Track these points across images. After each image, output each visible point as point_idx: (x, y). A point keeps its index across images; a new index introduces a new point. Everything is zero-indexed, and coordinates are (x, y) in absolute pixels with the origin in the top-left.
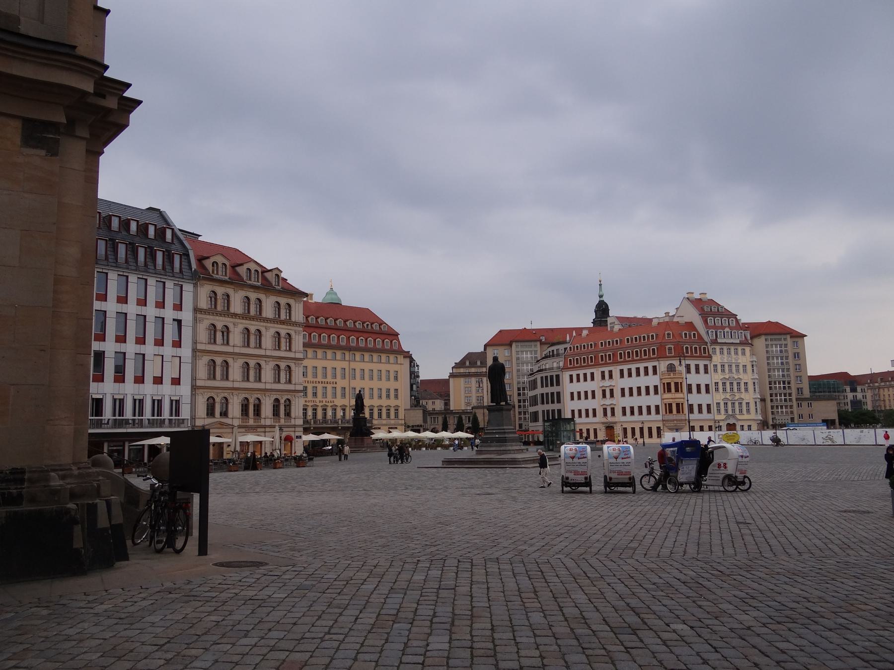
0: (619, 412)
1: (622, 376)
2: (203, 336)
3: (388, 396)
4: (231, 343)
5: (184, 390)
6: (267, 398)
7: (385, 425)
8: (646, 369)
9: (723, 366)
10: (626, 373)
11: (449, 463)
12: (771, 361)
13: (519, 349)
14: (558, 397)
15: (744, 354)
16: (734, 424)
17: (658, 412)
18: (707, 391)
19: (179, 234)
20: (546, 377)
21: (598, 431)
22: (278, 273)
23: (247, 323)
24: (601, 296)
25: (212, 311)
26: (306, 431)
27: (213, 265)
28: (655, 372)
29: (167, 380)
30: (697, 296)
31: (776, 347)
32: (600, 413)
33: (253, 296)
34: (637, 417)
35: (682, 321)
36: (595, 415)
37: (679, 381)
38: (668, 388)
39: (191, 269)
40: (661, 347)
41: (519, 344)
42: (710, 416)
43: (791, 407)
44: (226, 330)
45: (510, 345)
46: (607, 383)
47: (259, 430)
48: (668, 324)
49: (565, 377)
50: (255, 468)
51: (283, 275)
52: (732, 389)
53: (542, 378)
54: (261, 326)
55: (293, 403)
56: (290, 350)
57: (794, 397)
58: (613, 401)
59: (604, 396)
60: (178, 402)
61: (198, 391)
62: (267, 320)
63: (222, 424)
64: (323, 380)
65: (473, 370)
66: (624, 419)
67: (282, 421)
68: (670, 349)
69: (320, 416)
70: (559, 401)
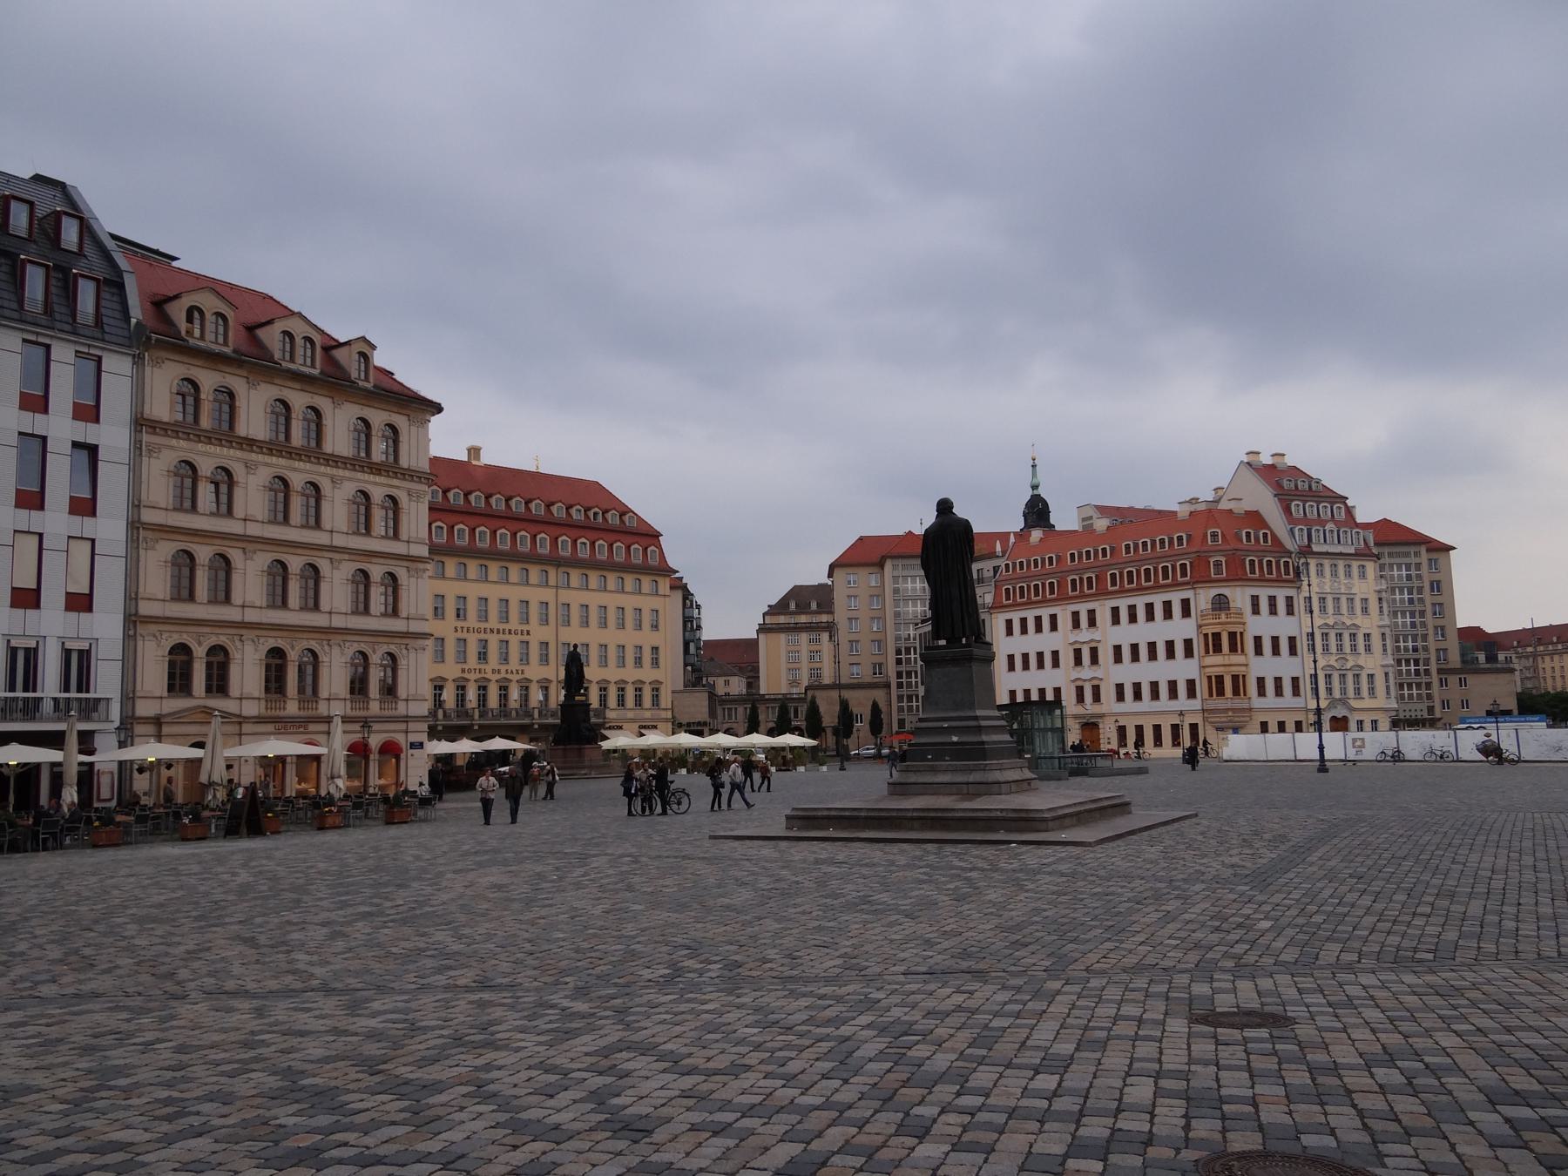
0: (1108, 693)
1: (1116, 620)
2: (159, 488)
3: (638, 662)
4: (239, 510)
5: (104, 627)
6: (336, 651)
7: (633, 720)
10: (1141, 613)
11: (810, 823)
13: (899, 572)
15: (1363, 575)
16: (1345, 719)
17: (1191, 693)
19: (110, 244)
22: (366, 349)
23: (280, 464)
24: (1035, 487)
25: (187, 429)
26: (434, 734)
27: (190, 319)
28: (1186, 612)
29: (53, 597)
30: (1266, 459)
31: (1399, 569)
33: (299, 400)
34: (1146, 704)
37: (1238, 629)
38: (1213, 644)
39: (127, 318)
40: (1200, 561)
41: (900, 562)
43: (1429, 686)
44: (225, 480)
46: (1085, 634)
47: (312, 727)
48: (1208, 516)
50: (256, 830)
51: (379, 359)
52: (1340, 648)
54: (321, 474)
55: (402, 662)
56: (396, 536)
57: (1433, 668)
58: (1097, 672)
59: (1078, 661)
60: (85, 656)
61: (140, 629)
62: (334, 460)
63: (208, 712)
64: (501, 627)
65: (803, 619)
67: (374, 708)
68: (1218, 564)
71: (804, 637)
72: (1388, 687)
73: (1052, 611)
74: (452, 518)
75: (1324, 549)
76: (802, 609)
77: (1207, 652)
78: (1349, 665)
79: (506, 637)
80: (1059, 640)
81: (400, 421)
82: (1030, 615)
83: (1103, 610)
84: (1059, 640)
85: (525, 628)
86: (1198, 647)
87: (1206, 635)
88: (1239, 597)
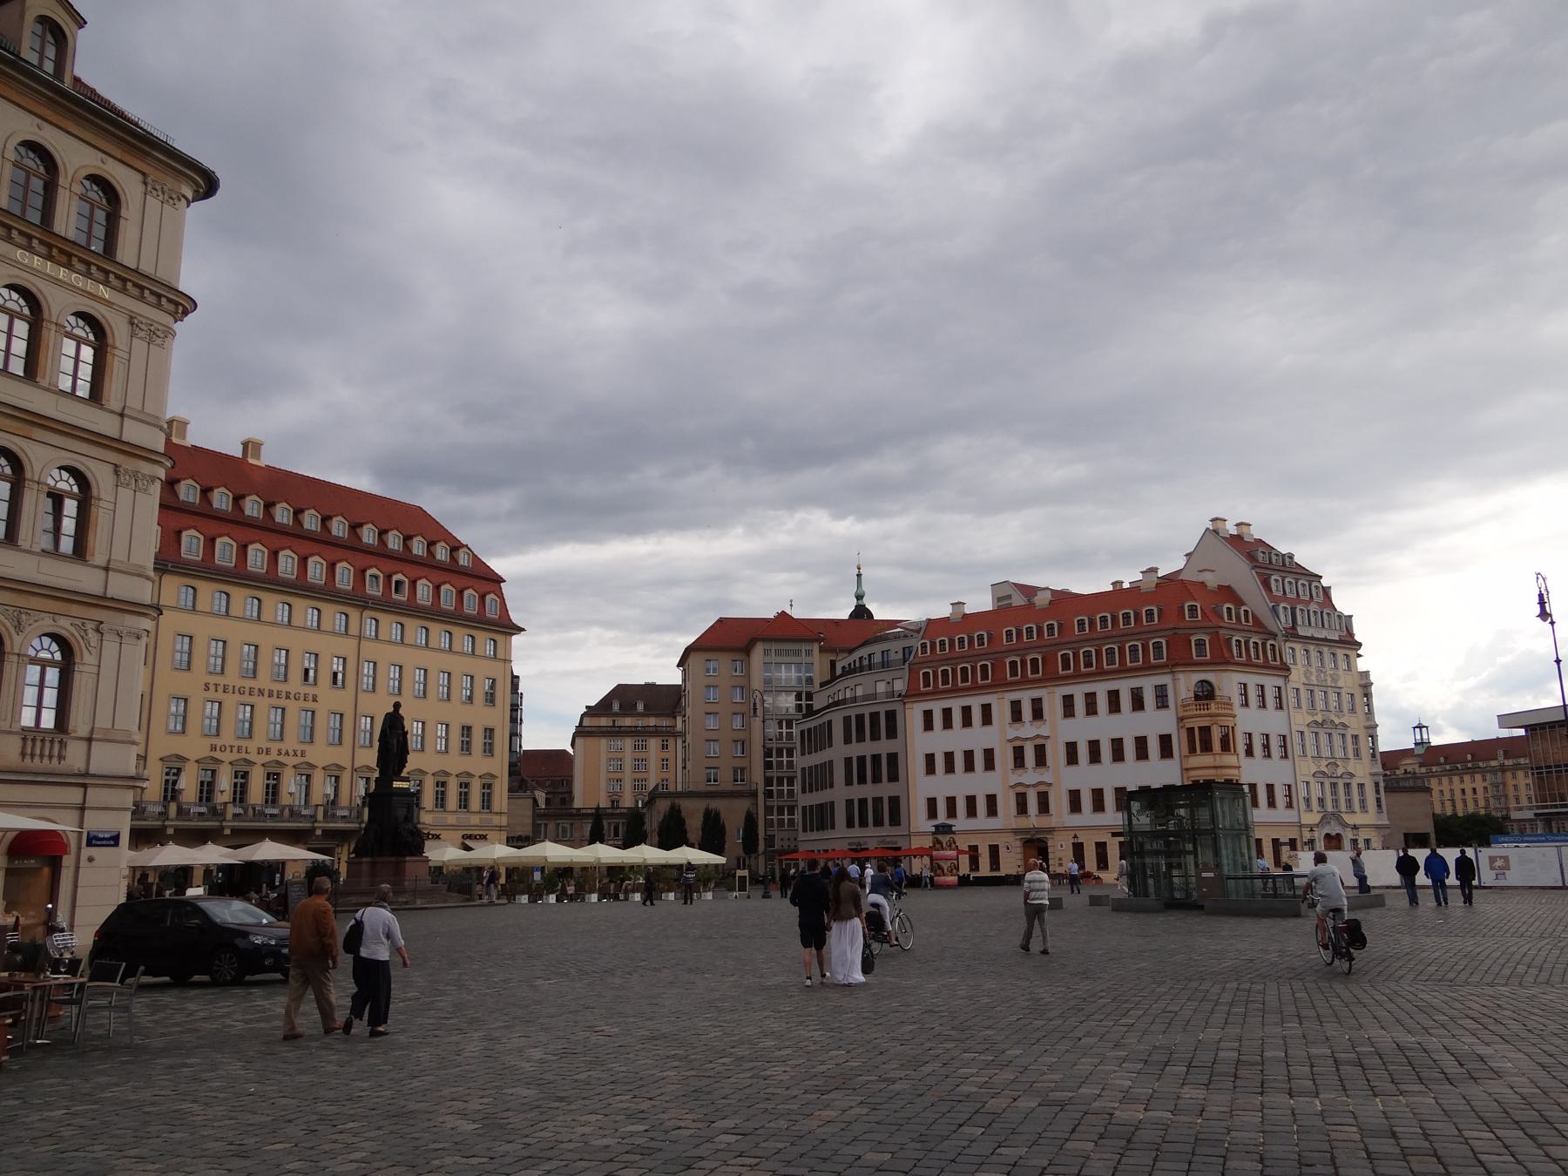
0: (1058, 802)
14: (893, 767)
16: (1338, 837)
20: (860, 718)
21: (1002, 851)
24: (859, 597)
28: (1162, 700)
32: (1007, 804)
35: (1212, 581)
36: (992, 810)
38: (1201, 740)
41: (774, 646)
42: (1290, 816)
45: (747, 650)
46: (1028, 729)
49: (913, 715)
53: (847, 720)
59: (1019, 760)
64: (276, 687)
65: (628, 722)
66: (1076, 820)
69: (256, 793)
70: (893, 777)
71: (628, 743)
72: (1378, 800)
73: (985, 699)
74: (213, 527)
75: (1308, 632)
76: (626, 711)
77: (1192, 750)
78: (1340, 771)
79: (283, 702)
80: (997, 736)
81: (126, 180)
82: (956, 705)
83: (1052, 699)
84: (997, 736)
85: (310, 690)
87: (1191, 731)
88: (1228, 683)
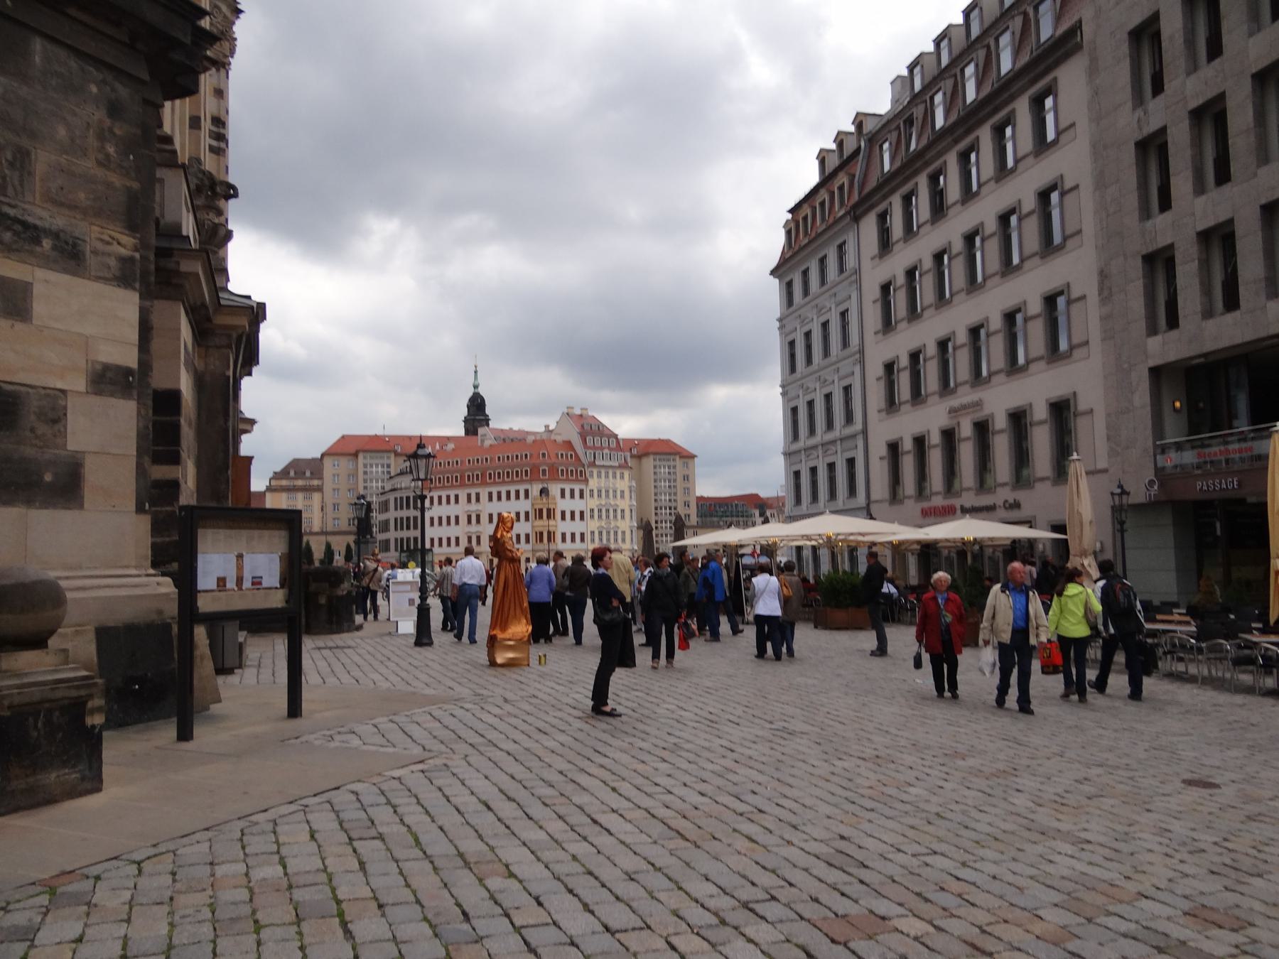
1: (490, 499)
8: (517, 492)
9: (600, 491)
12: (658, 484)
13: (368, 461)
15: (622, 477)
18: (582, 518)
24: (476, 387)
28: (527, 496)
30: (578, 412)
35: (559, 439)
37: (552, 507)
41: (368, 455)
45: (356, 455)
46: (474, 507)
48: (542, 443)
52: (608, 517)
58: (479, 528)
59: (469, 522)
65: (300, 483)
68: (544, 471)
80: (460, 509)
84: (460, 509)
86: (531, 516)
